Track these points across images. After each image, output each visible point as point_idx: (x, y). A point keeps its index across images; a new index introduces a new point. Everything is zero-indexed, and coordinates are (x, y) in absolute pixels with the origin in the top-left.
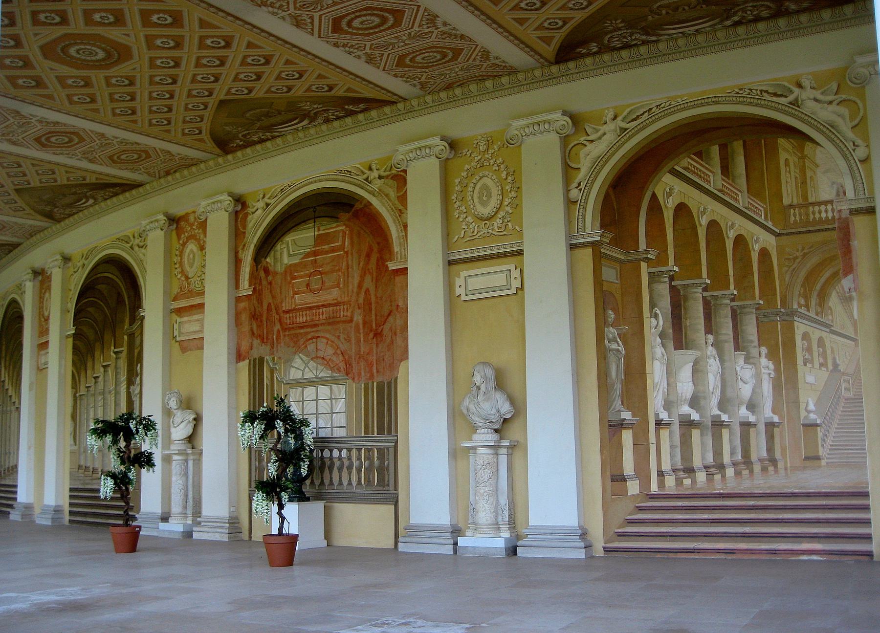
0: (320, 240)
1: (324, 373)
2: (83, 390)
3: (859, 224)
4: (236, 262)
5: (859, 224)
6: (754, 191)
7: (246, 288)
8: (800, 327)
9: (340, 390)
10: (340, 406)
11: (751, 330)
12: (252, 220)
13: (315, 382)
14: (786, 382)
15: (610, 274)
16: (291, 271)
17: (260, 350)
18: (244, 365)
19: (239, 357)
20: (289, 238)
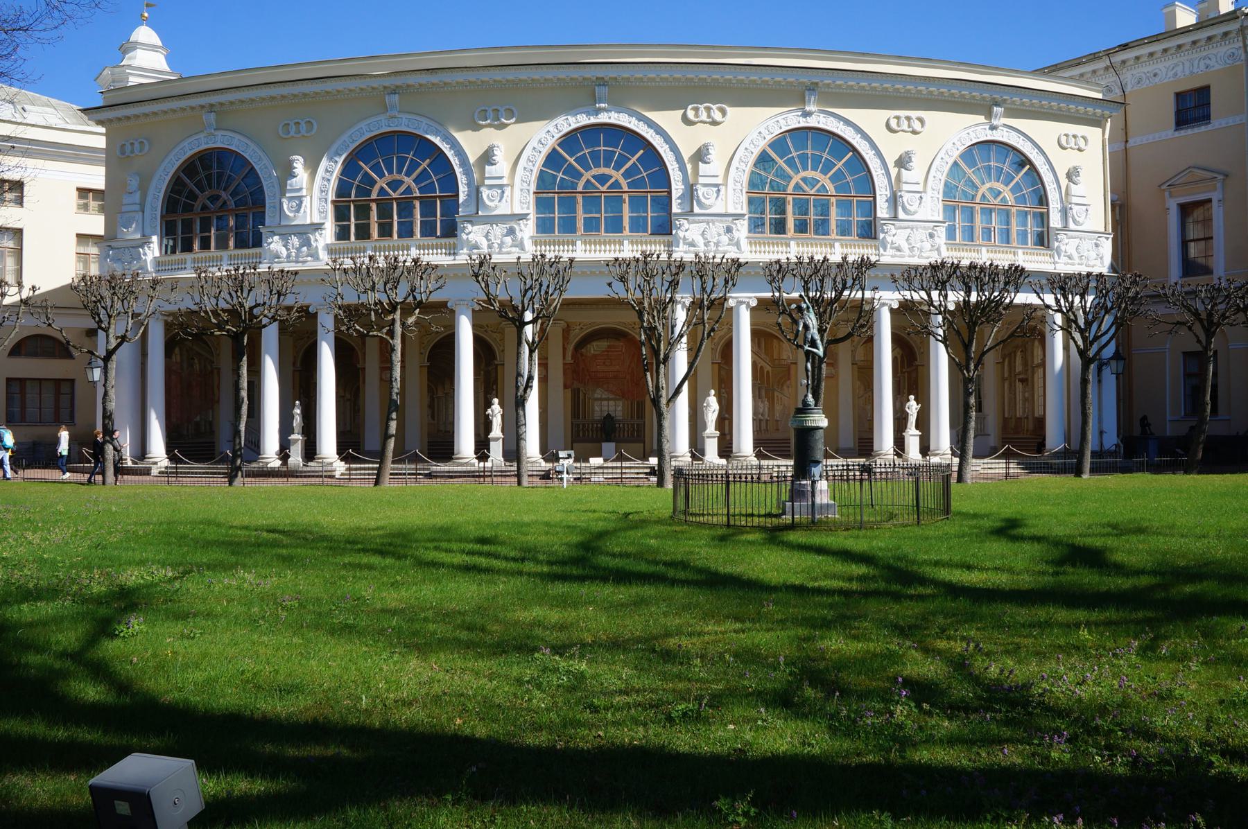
0: (609, 347)
1: (611, 396)
2: (440, 394)
3: (793, 366)
4: (564, 349)
5: (793, 366)
6: (766, 354)
7: (569, 359)
8: (776, 394)
9: (620, 403)
10: (620, 408)
11: (763, 393)
12: (572, 333)
13: (608, 399)
14: (772, 408)
15: (723, 373)
16: (595, 356)
17: (576, 385)
18: (569, 392)
19: (565, 387)
20: (595, 344)
